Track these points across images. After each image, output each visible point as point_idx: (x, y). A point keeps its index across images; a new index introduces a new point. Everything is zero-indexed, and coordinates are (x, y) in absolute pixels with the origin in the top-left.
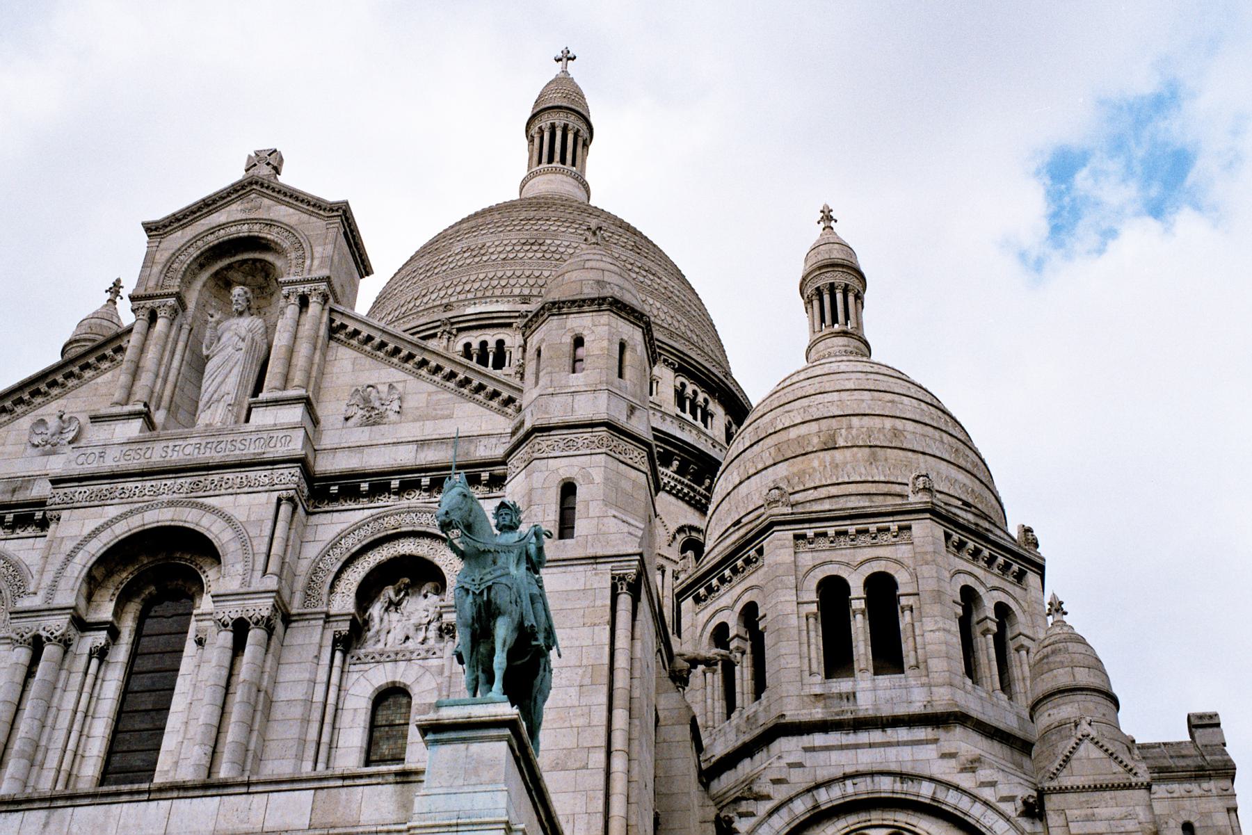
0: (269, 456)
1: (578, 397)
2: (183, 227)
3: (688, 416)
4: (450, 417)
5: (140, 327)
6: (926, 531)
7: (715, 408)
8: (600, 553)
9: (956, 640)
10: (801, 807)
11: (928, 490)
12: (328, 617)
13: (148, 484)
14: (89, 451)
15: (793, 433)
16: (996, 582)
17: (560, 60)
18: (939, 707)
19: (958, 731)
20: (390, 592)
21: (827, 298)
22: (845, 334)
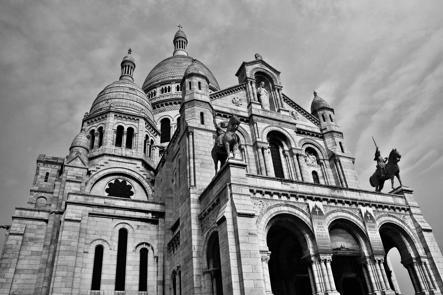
2: (251, 65)
4: (307, 122)
5: (249, 84)
8: (350, 157)
12: (305, 157)
13: (271, 121)
14: (256, 110)
17: (180, 27)
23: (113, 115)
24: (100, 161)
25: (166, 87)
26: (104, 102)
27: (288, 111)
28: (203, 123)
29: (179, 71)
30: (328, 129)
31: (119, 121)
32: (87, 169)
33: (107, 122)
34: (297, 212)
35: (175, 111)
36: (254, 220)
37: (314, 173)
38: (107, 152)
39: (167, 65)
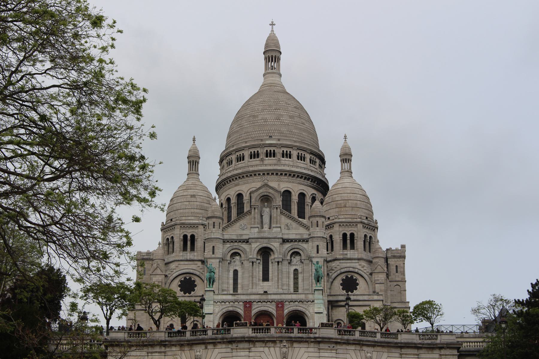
0: (278, 237)
1: (319, 232)
3: (312, 165)
6: (360, 226)
7: (318, 161)
9: (363, 245)
10: (339, 272)
11: (360, 218)
12: (287, 260)
15: (339, 202)
16: (370, 232)
18: (360, 257)
19: (362, 261)
20: (294, 256)
21: (345, 161)
22: (348, 171)
23: (179, 227)
24: (173, 266)
25: (240, 155)
26: (172, 213)
27: (280, 227)
28: (213, 253)
29: (254, 130)
30: (312, 236)
31: (184, 231)
32: (165, 275)
33: (175, 233)
34: (237, 309)
35: (247, 184)
36: (212, 315)
37: (296, 270)
38: (177, 258)
39: (244, 120)
